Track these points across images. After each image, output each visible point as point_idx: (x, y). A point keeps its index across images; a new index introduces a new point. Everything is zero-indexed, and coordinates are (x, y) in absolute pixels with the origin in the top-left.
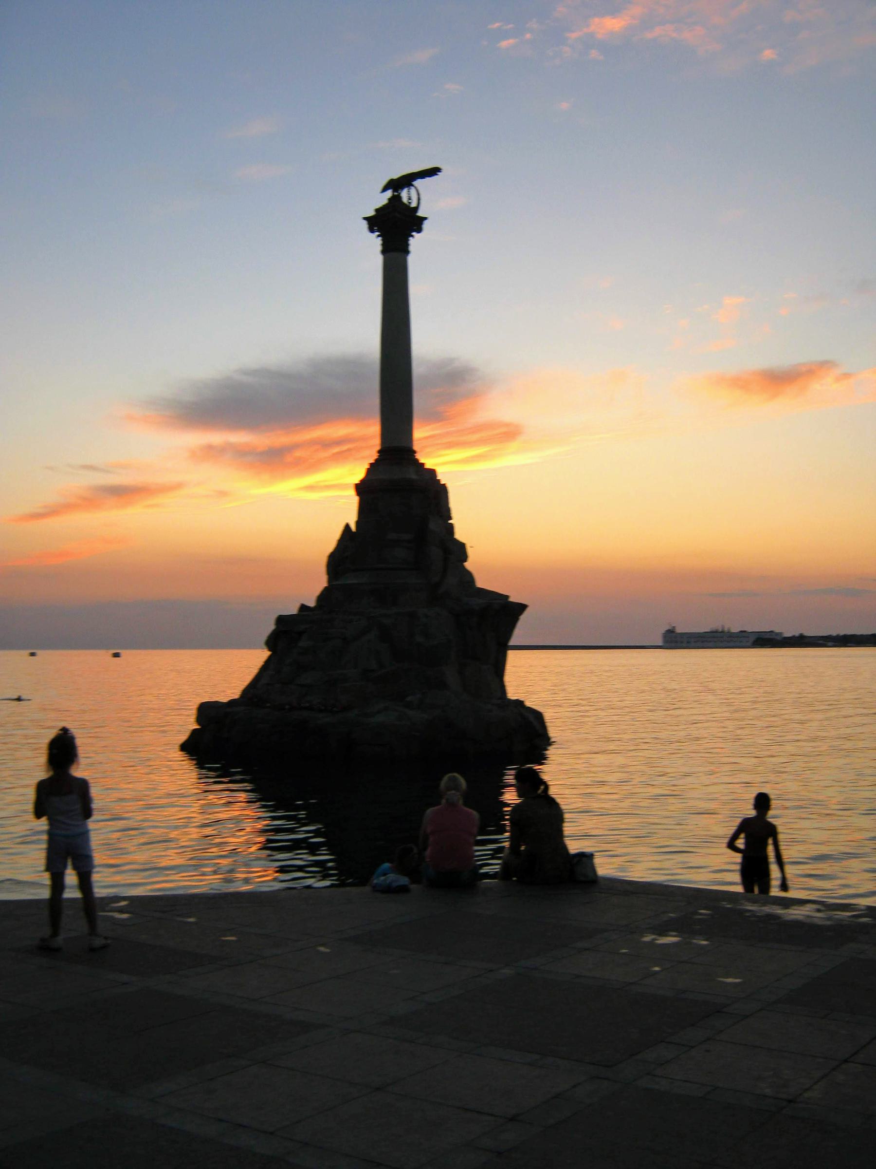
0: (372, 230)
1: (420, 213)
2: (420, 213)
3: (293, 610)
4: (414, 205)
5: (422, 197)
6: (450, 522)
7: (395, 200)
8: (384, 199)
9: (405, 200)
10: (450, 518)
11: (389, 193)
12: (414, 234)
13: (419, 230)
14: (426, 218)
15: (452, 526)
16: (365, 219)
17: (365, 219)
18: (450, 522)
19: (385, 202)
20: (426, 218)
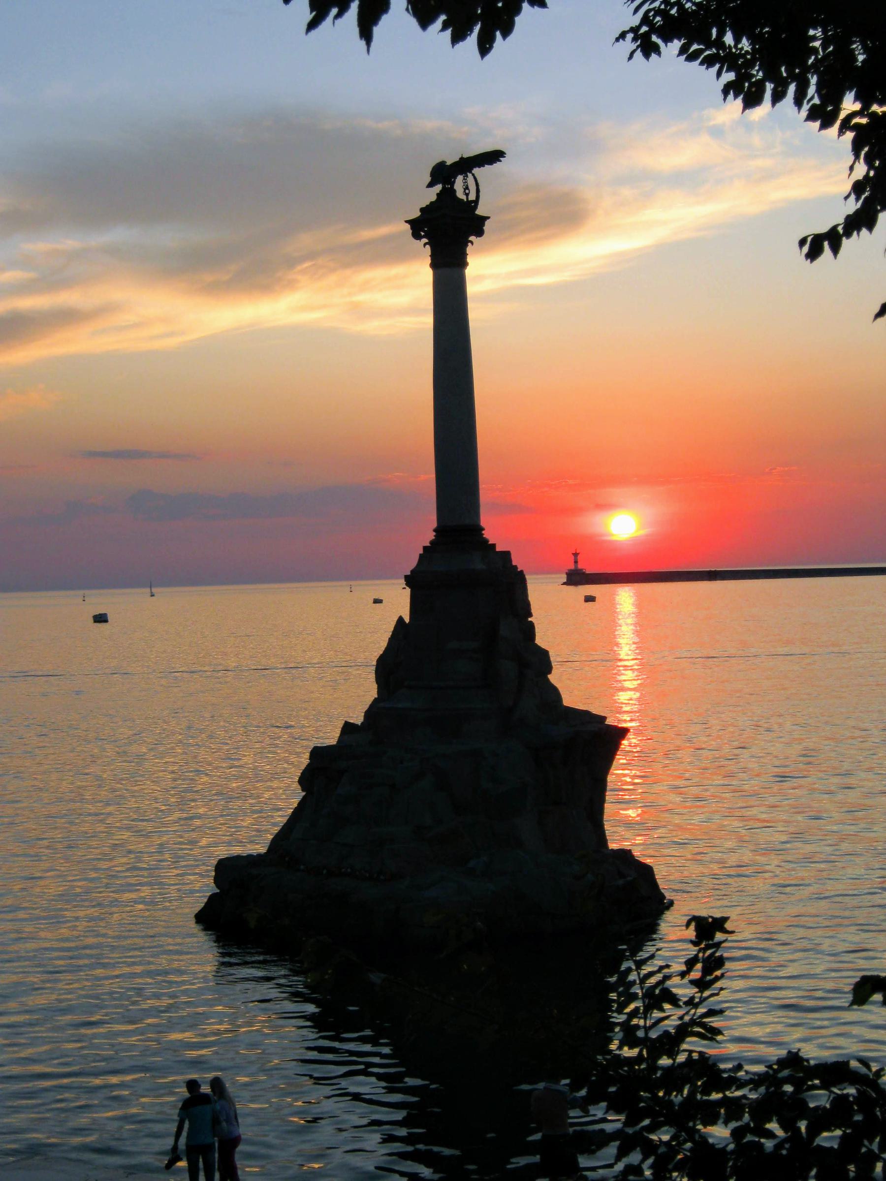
0: (416, 236)
1: (480, 211)
2: (480, 211)
3: (331, 737)
4: (472, 197)
5: (481, 188)
6: (530, 619)
7: (447, 194)
8: (431, 195)
9: (460, 194)
10: (531, 615)
11: (438, 188)
12: (472, 238)
13: (480, 233)
14: (488, 218)
15: (532, 625)
16: (406, 222)
17: (406, 222)
18: (530, 619)
19: (434, 198)
20: (488, 218)
